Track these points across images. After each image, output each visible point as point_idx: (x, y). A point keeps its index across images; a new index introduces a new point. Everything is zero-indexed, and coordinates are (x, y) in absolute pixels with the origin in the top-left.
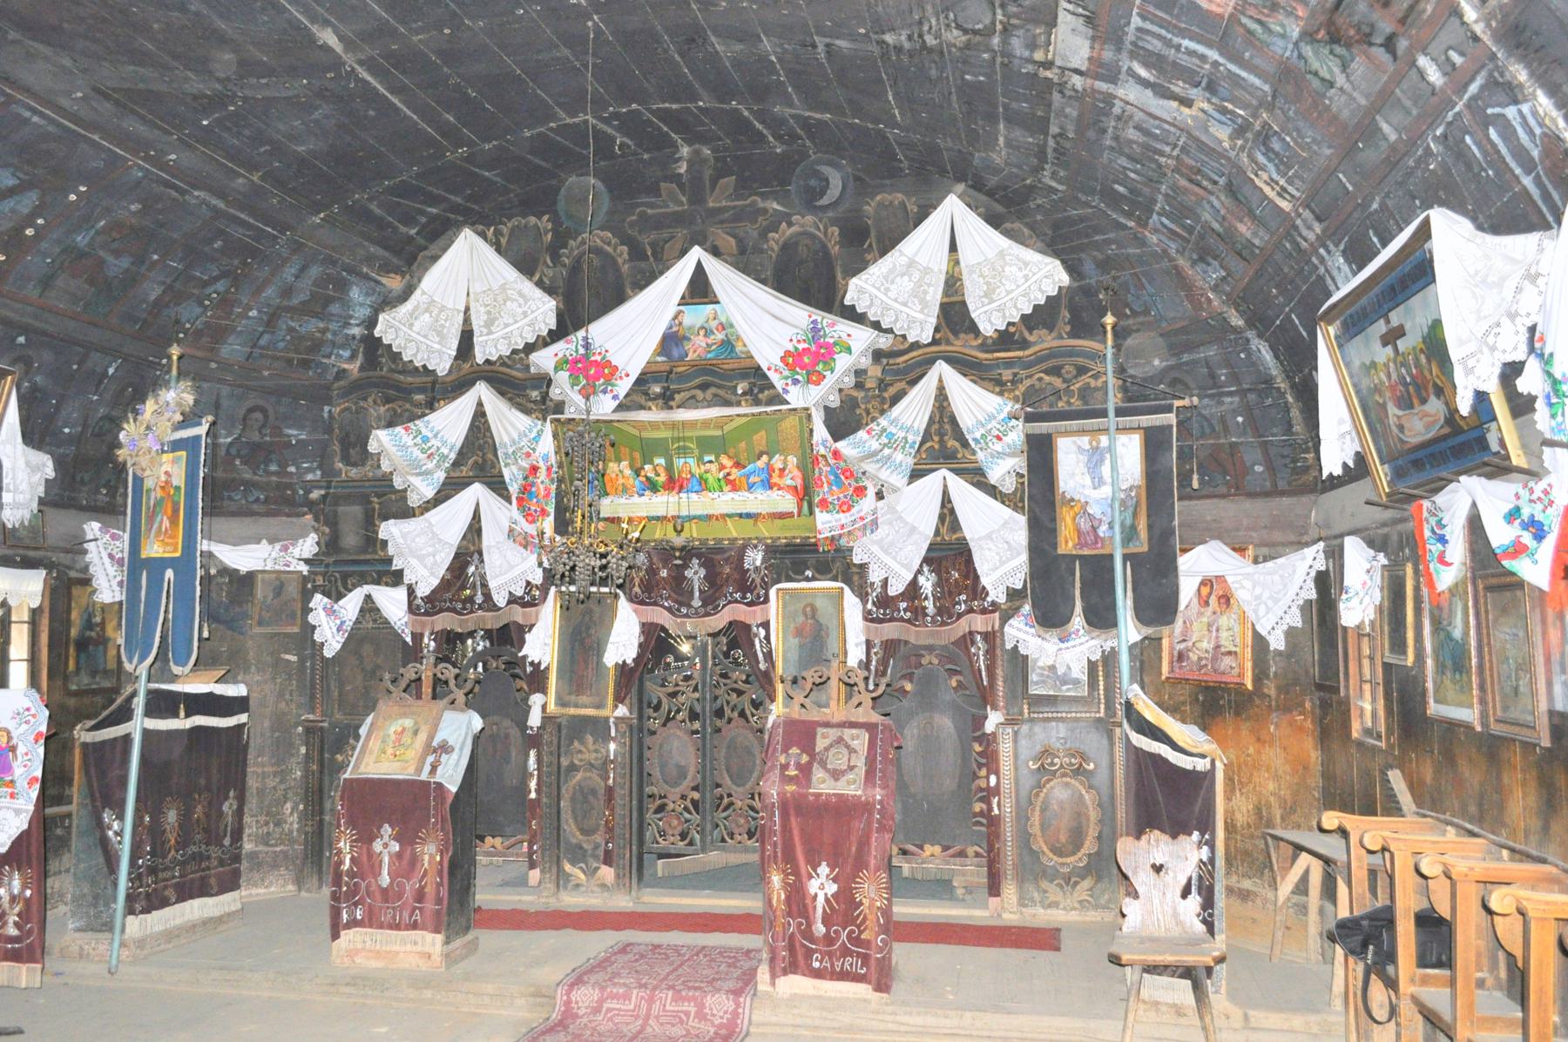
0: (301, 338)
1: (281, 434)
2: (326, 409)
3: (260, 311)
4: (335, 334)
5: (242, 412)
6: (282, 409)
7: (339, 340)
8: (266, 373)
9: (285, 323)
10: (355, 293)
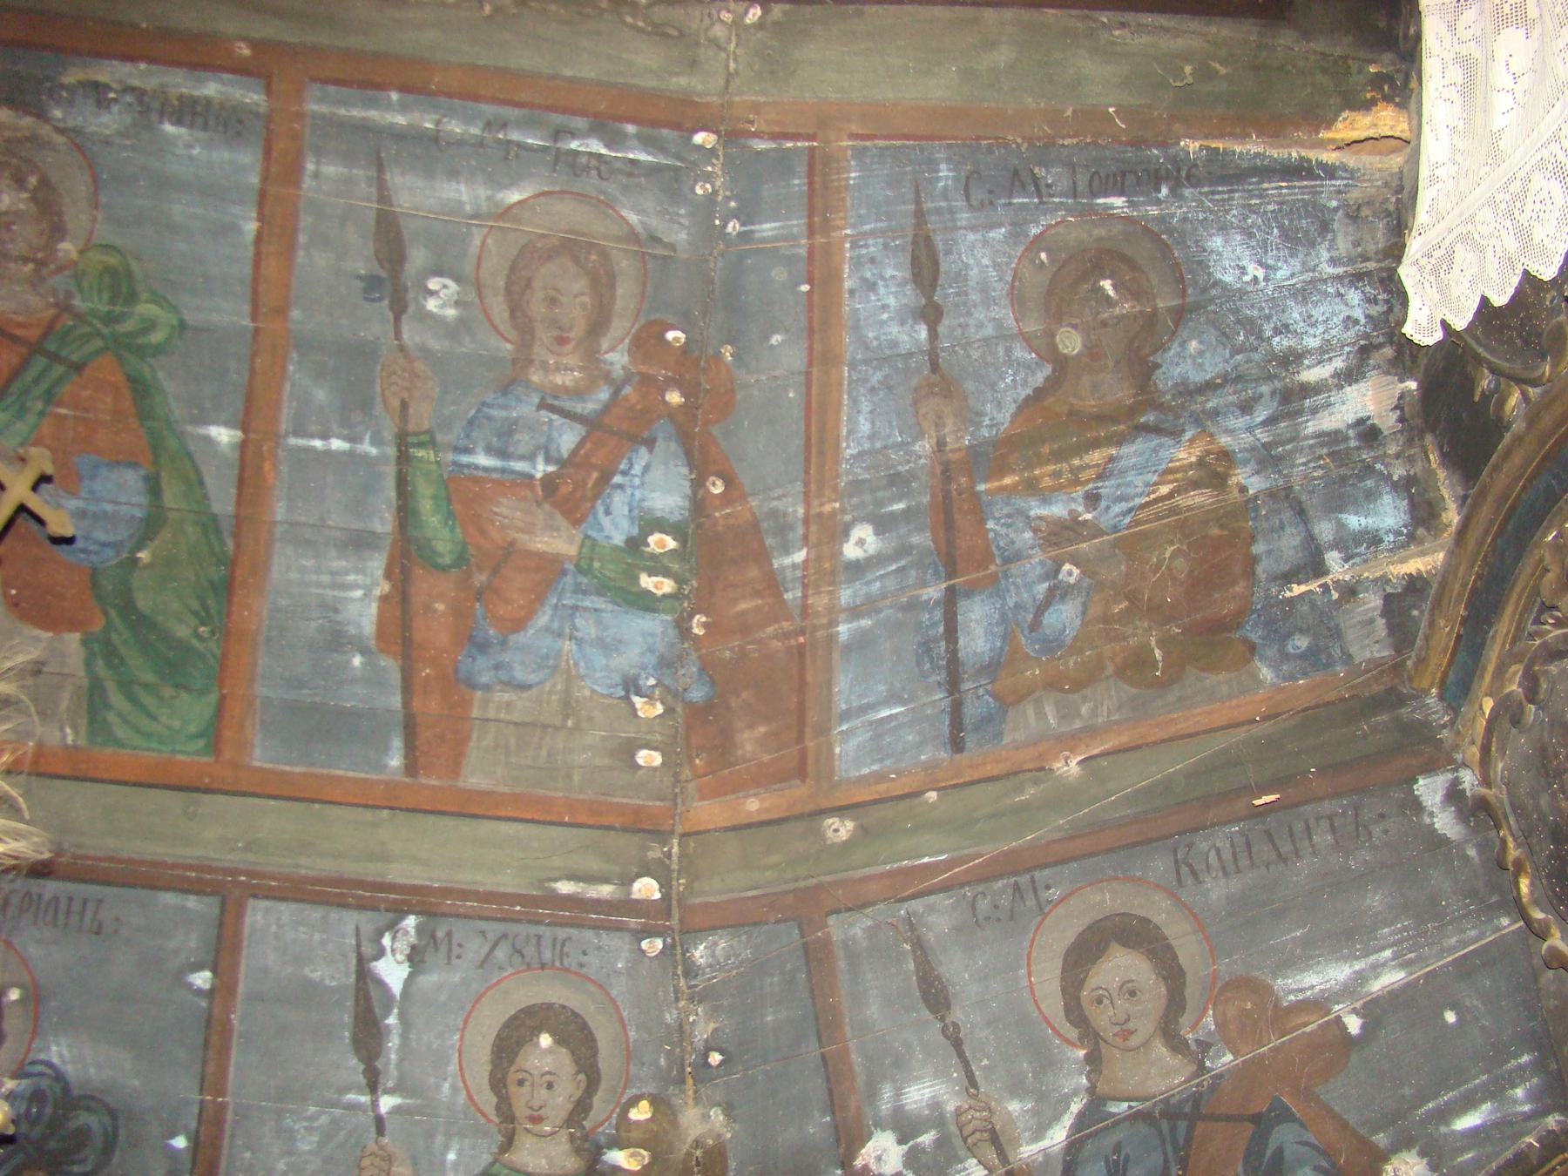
0: (1132, 545)
1: (1282, 1016)
2: (1430, 790)
3: (882, 525)
4: (1267, 458)
5: (1047, 979)
6: (1217, 890)
7: (1303, 469)
8: (1069, 767)
9: (1021, 516)
10: (1234, 260)
